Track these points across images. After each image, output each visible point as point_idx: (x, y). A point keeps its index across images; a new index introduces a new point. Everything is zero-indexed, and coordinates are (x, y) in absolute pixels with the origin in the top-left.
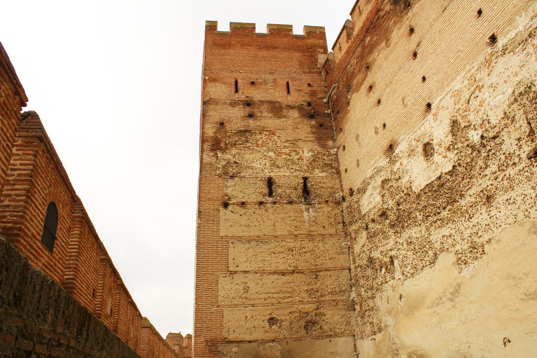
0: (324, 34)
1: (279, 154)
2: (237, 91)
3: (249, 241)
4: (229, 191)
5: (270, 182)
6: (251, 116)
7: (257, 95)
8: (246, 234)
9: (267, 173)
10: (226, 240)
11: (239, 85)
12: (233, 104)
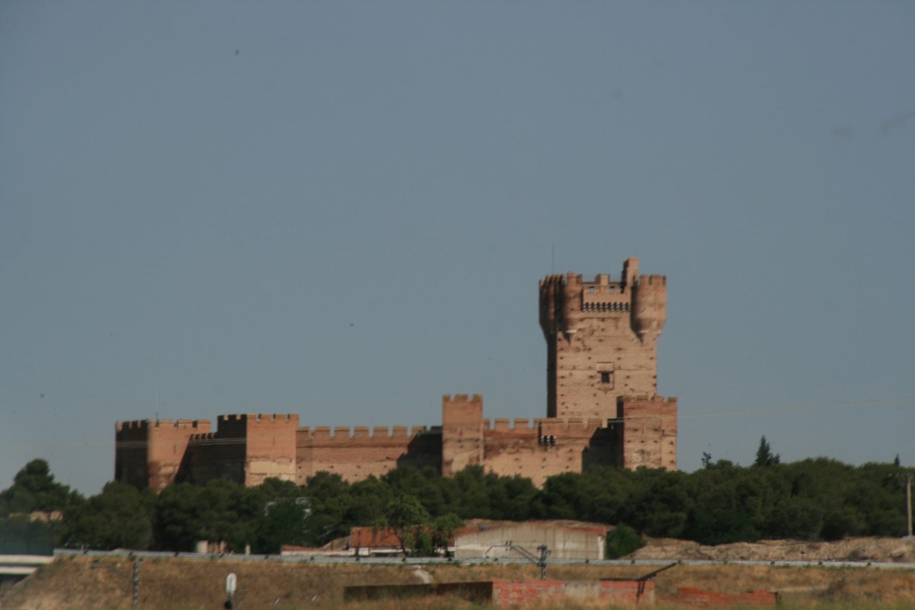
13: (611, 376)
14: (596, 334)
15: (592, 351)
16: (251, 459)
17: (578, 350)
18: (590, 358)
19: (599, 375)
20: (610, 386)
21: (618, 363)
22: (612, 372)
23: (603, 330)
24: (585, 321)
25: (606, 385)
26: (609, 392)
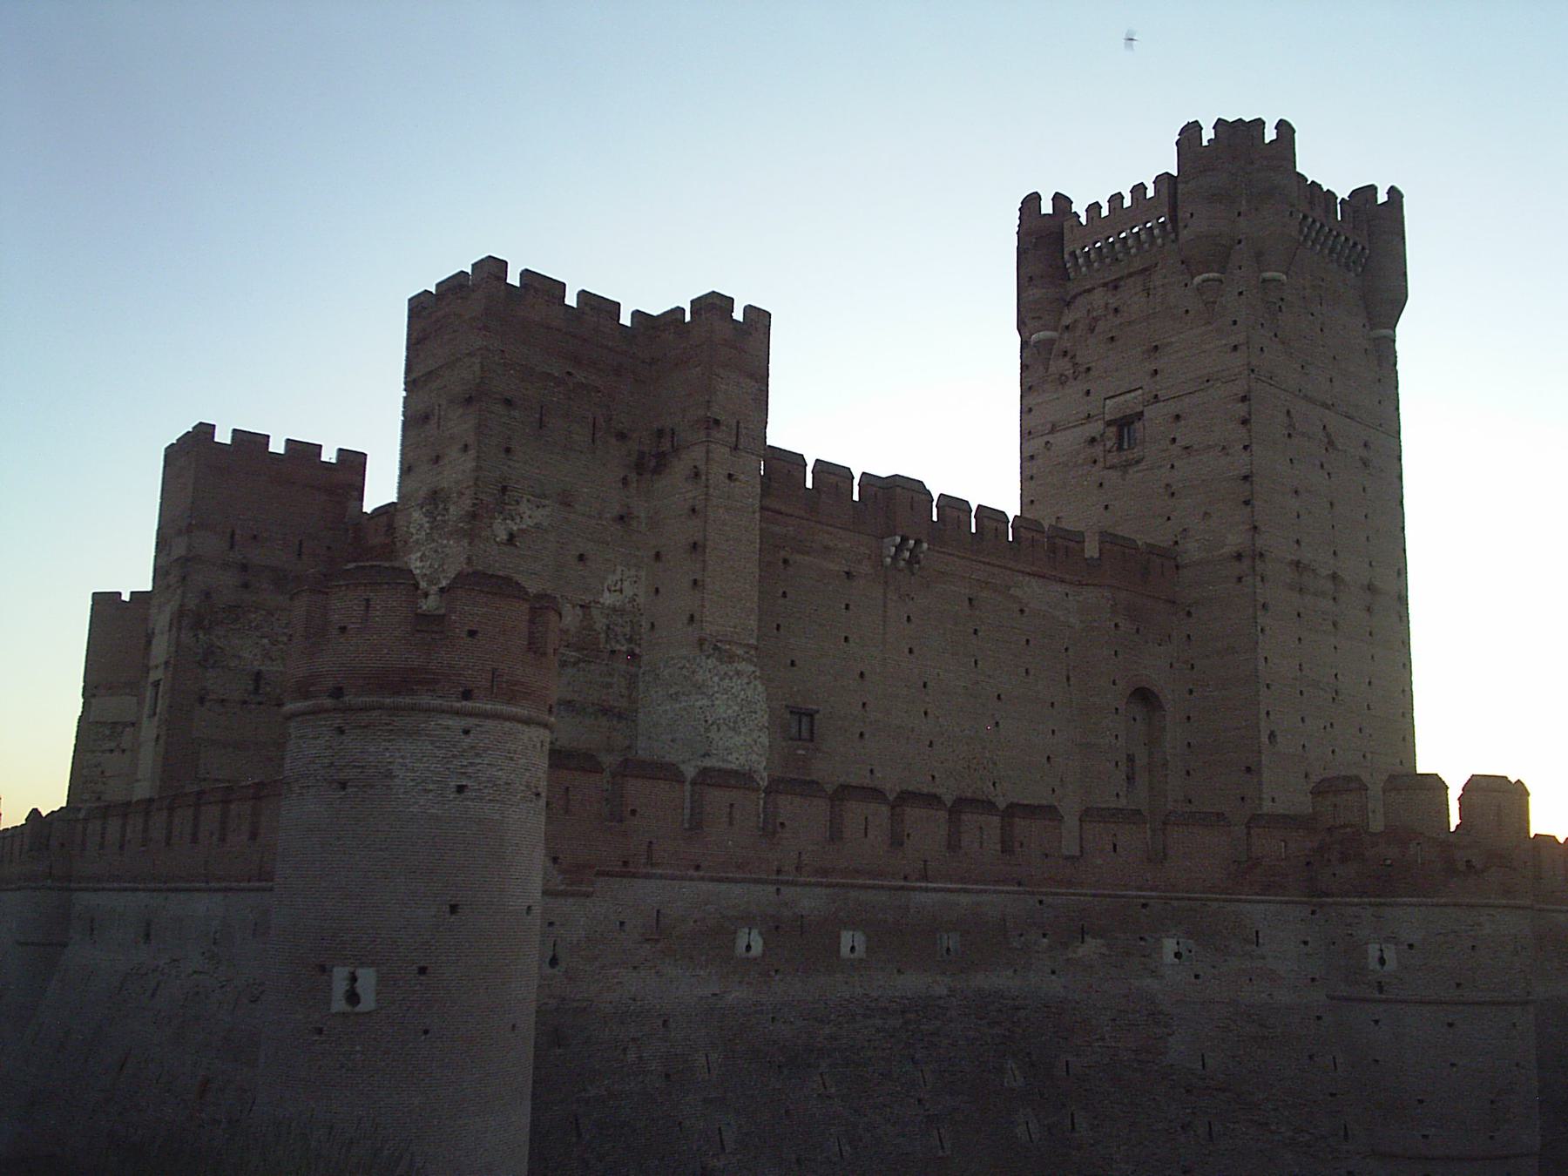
2: (232, 547)
6: (246, 586)
11: (237, 537)
14: (1101, 327)
17: (1062, 380)
18: (1088, 393)
19: (1113, 429)
20: (1136, 453)
23: (1116, 310)
24: (1080, 301)
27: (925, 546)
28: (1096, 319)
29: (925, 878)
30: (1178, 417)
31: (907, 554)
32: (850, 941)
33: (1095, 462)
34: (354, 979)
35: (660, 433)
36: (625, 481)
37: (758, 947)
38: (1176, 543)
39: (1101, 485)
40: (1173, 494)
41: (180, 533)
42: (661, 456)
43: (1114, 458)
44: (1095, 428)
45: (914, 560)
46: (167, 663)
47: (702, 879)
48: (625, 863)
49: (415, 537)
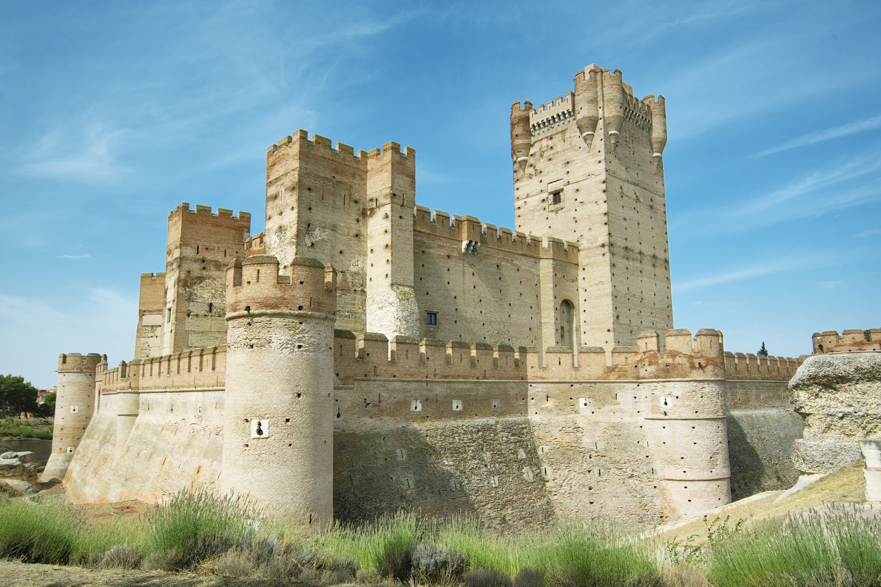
0: (249, 218)
1: (216, 291)
2: (198, 253)
3: (199, 333)
4: (191, 308)
5: (211, 305)
6: (204, 268)
7: (209, 256)
8: (197, 330)
9: (210, 301)
10: (188, 332)
11: (199, 250)
12: (196, 261)
13: (561, 194)
14: (546, 154)
15: (543, 173)
16: (144, 313)
17: (530, 176)
18: (541, 181)
19: (551, 197)
20: (561, 205)
21: (566, 178)
22: (562, 190)
23: (552, 148)
24: (536, 144)
25: (558, 206)
26: (560, 212)
27: (479, 244)
28: (543, 152)
29: (485, 378)
30: (577, 190)
31: (472, 248)
32: (457, 405)
33: (545, 209)
34: (260, 424)
35: (371, 200)
36: (358, 221)
37: (419, 408)
38: (578, 241)
39: (547, 218)
40: (576, 221)
41: (176, 248)
42: (372, 210)
43: (552, 207)
44: (544, 196)
45: (474, 250)
46: (174, 301)
47: (396, 381)
48: (366, 375)
49: (273, 246)
